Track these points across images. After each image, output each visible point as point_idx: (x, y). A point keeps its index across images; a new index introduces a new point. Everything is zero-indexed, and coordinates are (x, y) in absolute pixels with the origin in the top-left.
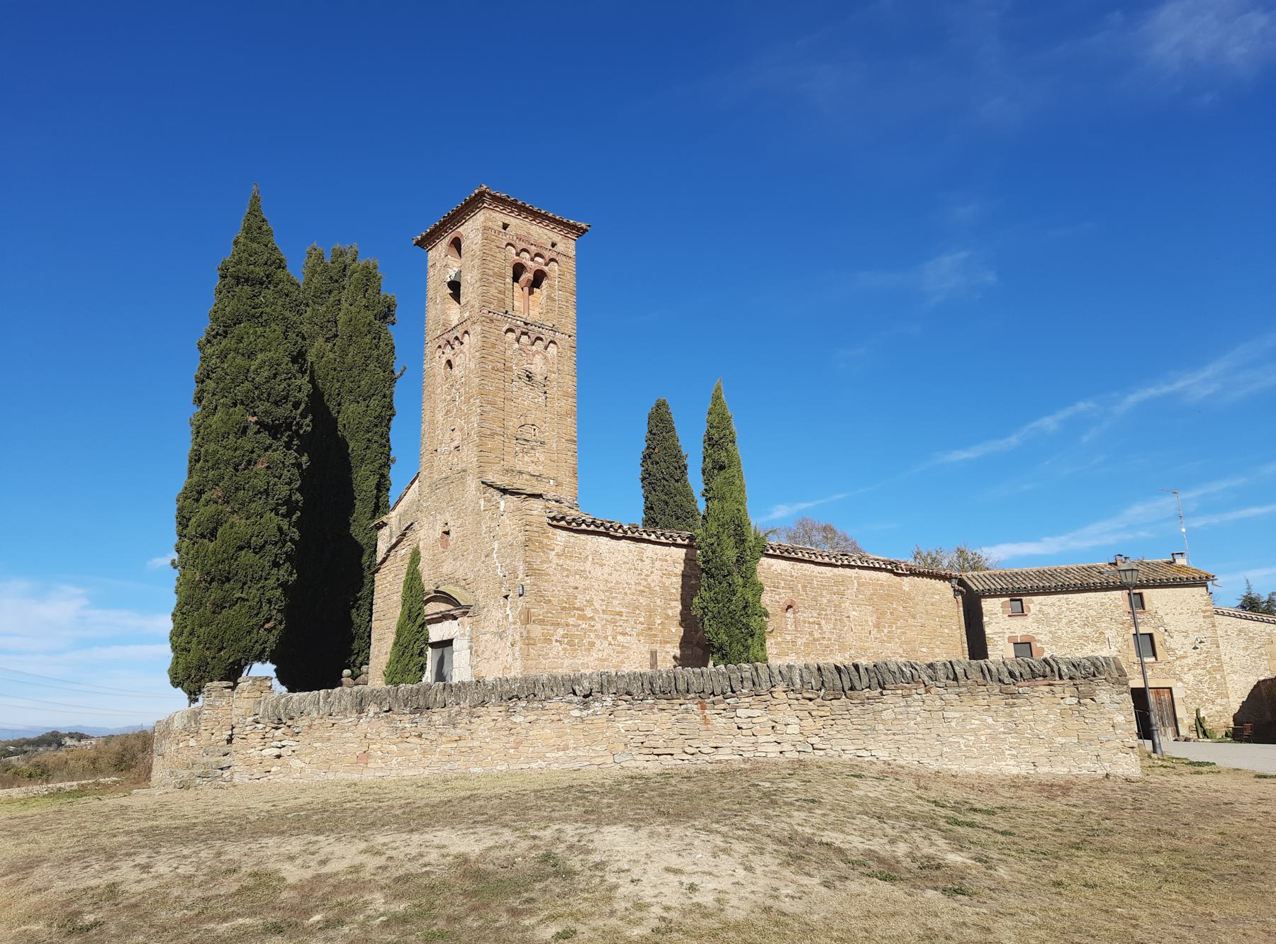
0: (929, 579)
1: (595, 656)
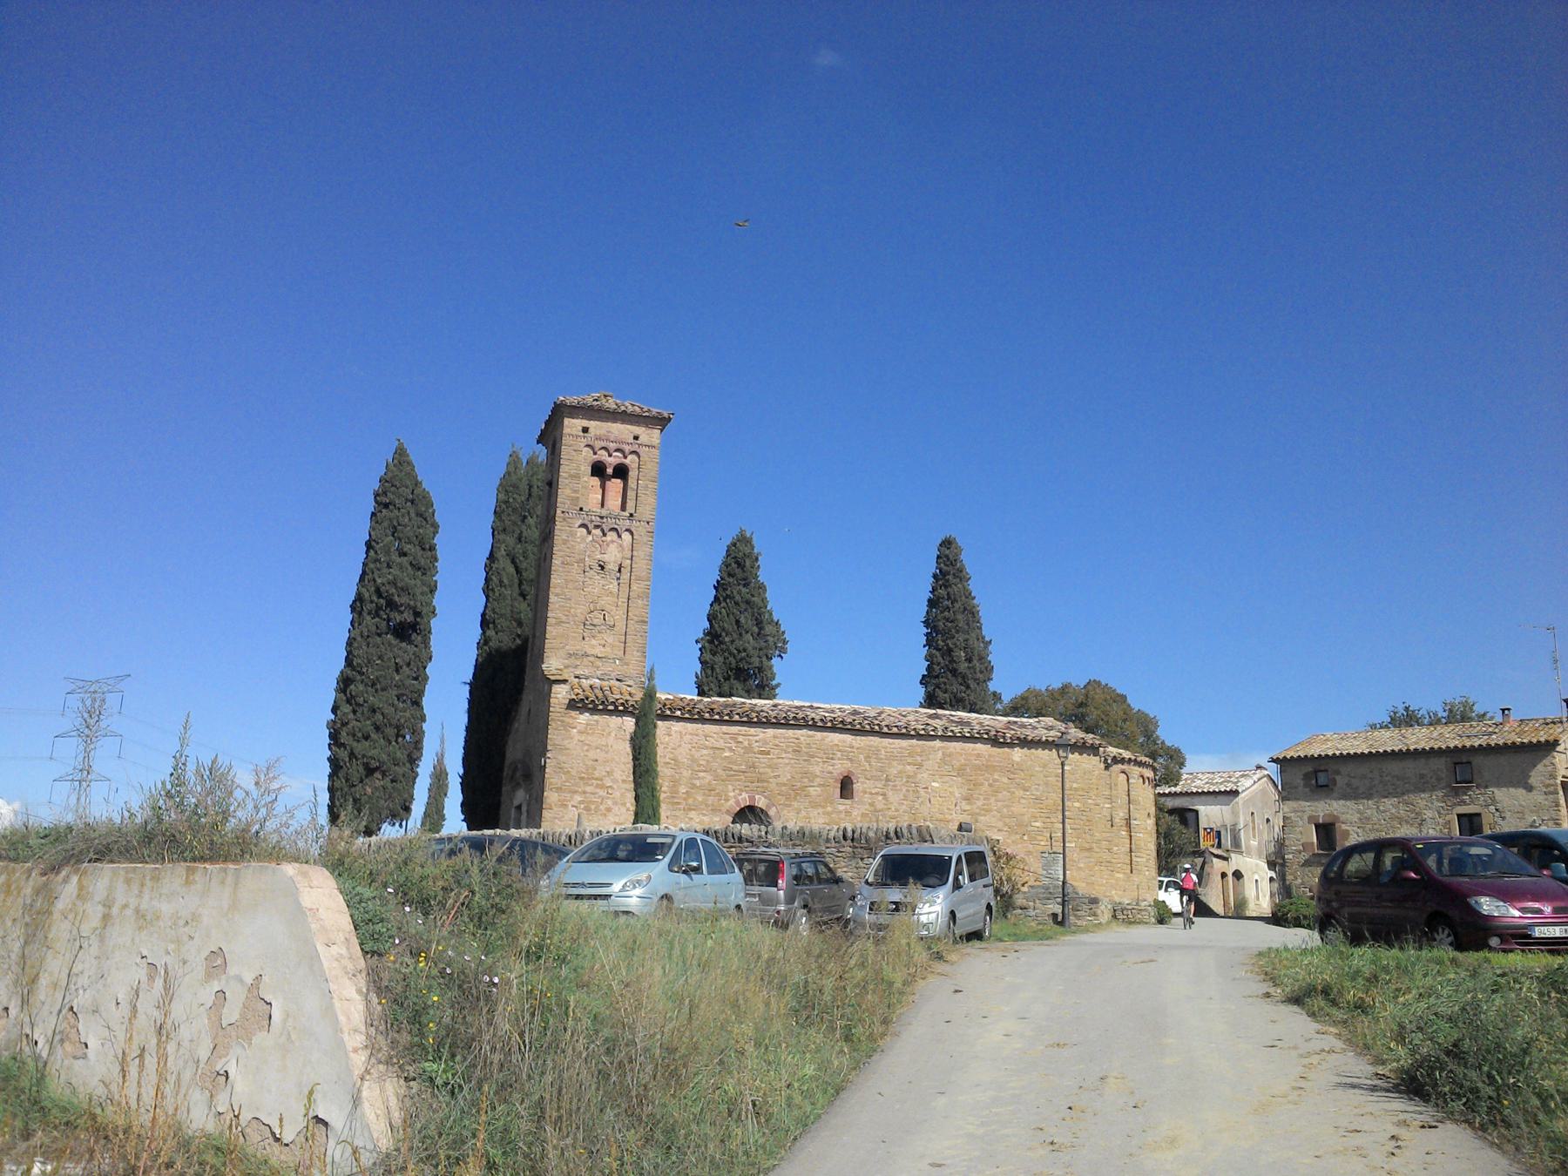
0: (1436, 747)
1: (612, 820)
